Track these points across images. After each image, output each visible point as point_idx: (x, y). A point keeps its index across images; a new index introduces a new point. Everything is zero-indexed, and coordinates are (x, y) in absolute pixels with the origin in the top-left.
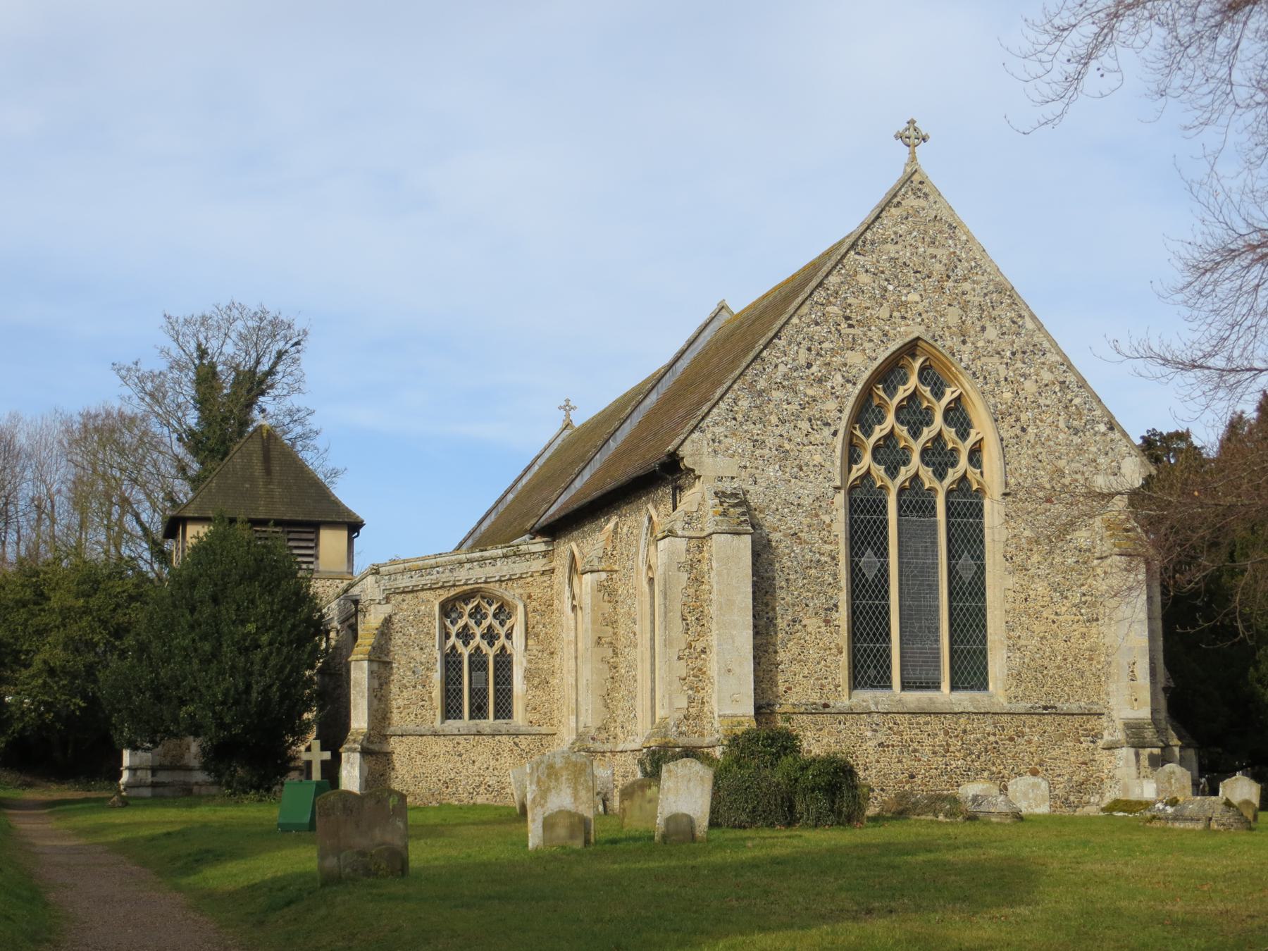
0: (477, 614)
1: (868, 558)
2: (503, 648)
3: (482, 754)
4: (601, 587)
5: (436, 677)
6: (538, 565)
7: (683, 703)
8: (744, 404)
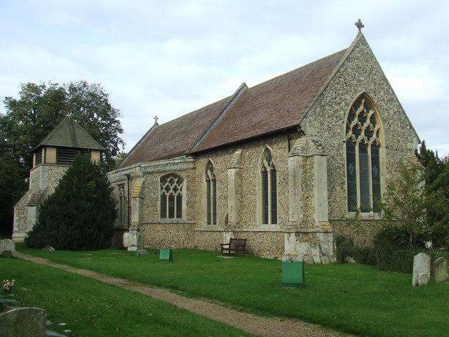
0: (171, 182)
1: (351, 166)
2: (179, 194)
3: (173, 231)
4: (237, 174)
5: (159, 203)
6: (191, 166)
7: (302, 216)
8: (318, 109)
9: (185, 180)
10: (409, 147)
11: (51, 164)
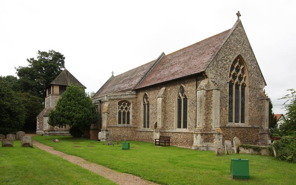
0: (124, 105)
2: (128, 111)
5: (117, 116)
6: (135, 96)
8: (215, 63)
9: (132, 105)
10: (260, 87)
11: (56, 95)
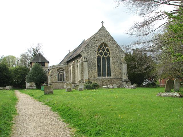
0: (61, 71)
5: (57, 77)
6: (67, 66)
8: (87, 49)
10: (121, 57)
